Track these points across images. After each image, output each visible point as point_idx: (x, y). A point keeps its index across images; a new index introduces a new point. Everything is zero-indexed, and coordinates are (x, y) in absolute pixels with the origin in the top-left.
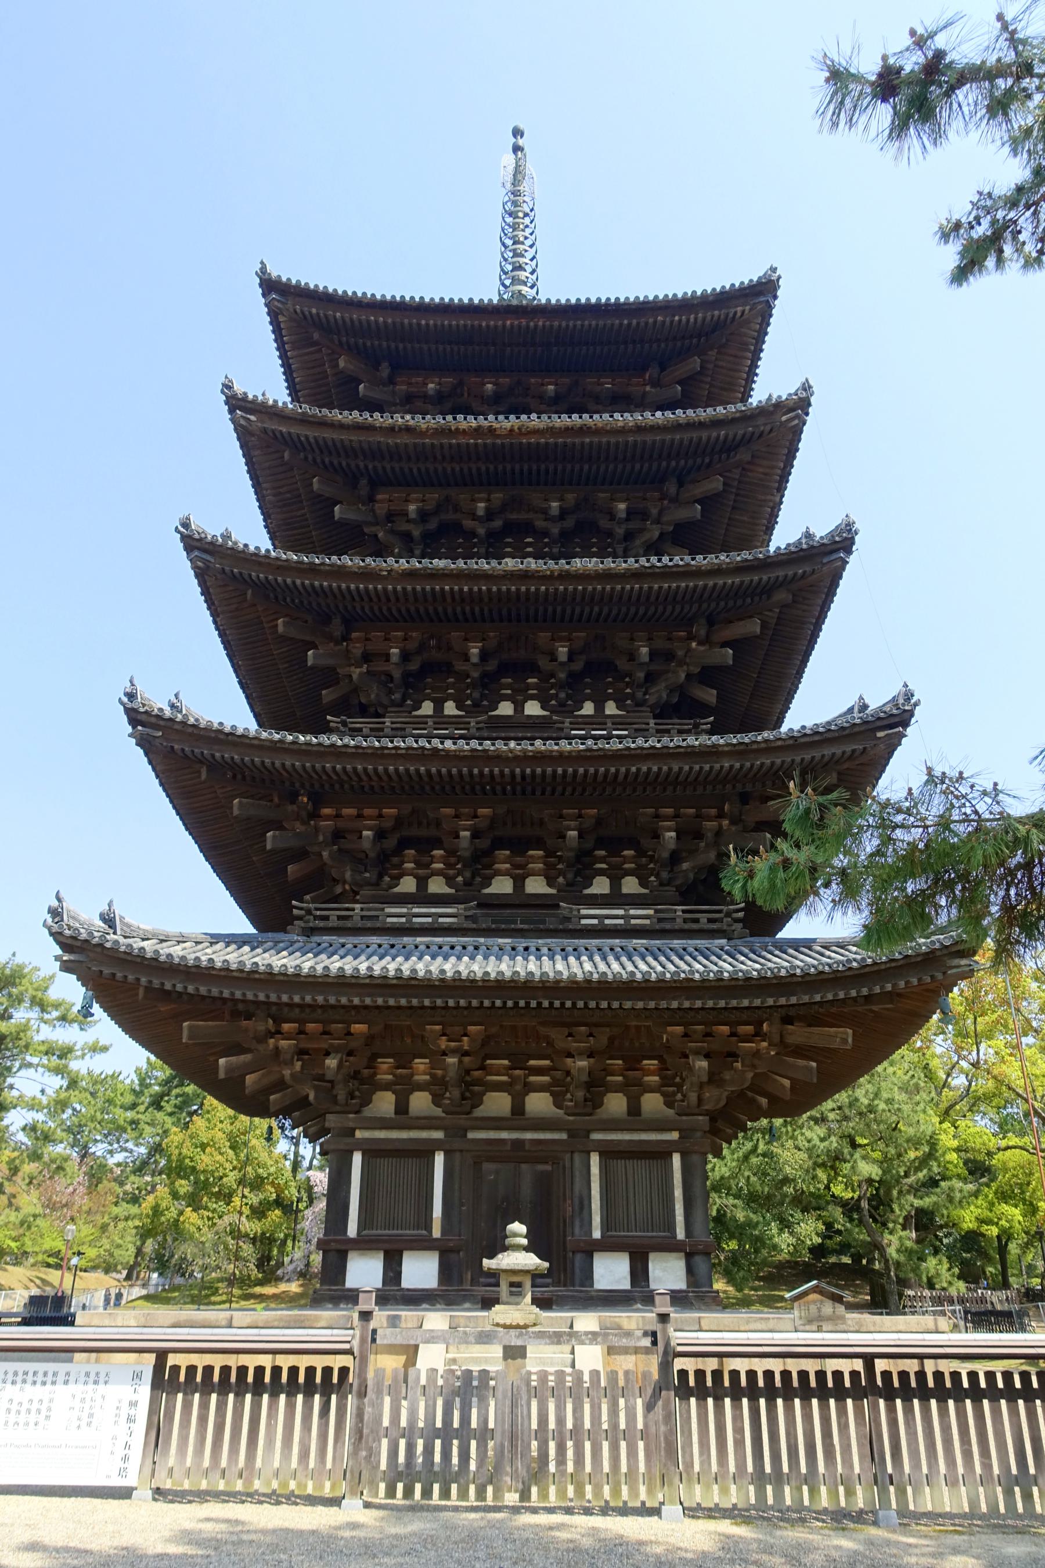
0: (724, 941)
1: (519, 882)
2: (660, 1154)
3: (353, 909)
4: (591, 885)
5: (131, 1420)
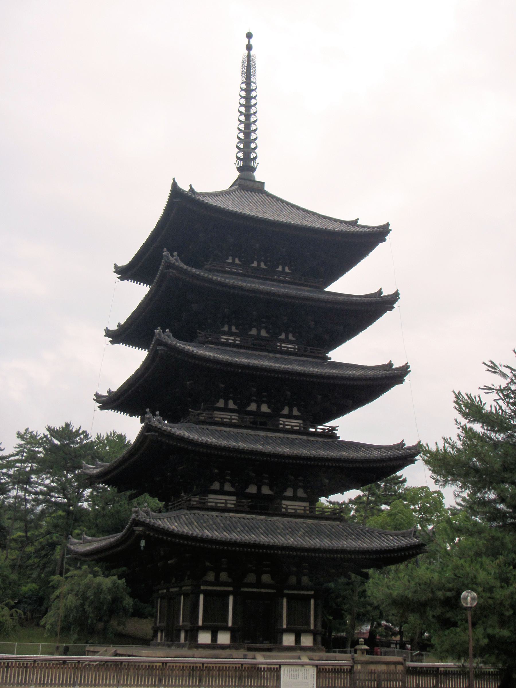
0: (338, 523)
1: (259, 489)
2: (307, 598)
3: (204, 499)
4: (285, 491)
5: (314, 678)
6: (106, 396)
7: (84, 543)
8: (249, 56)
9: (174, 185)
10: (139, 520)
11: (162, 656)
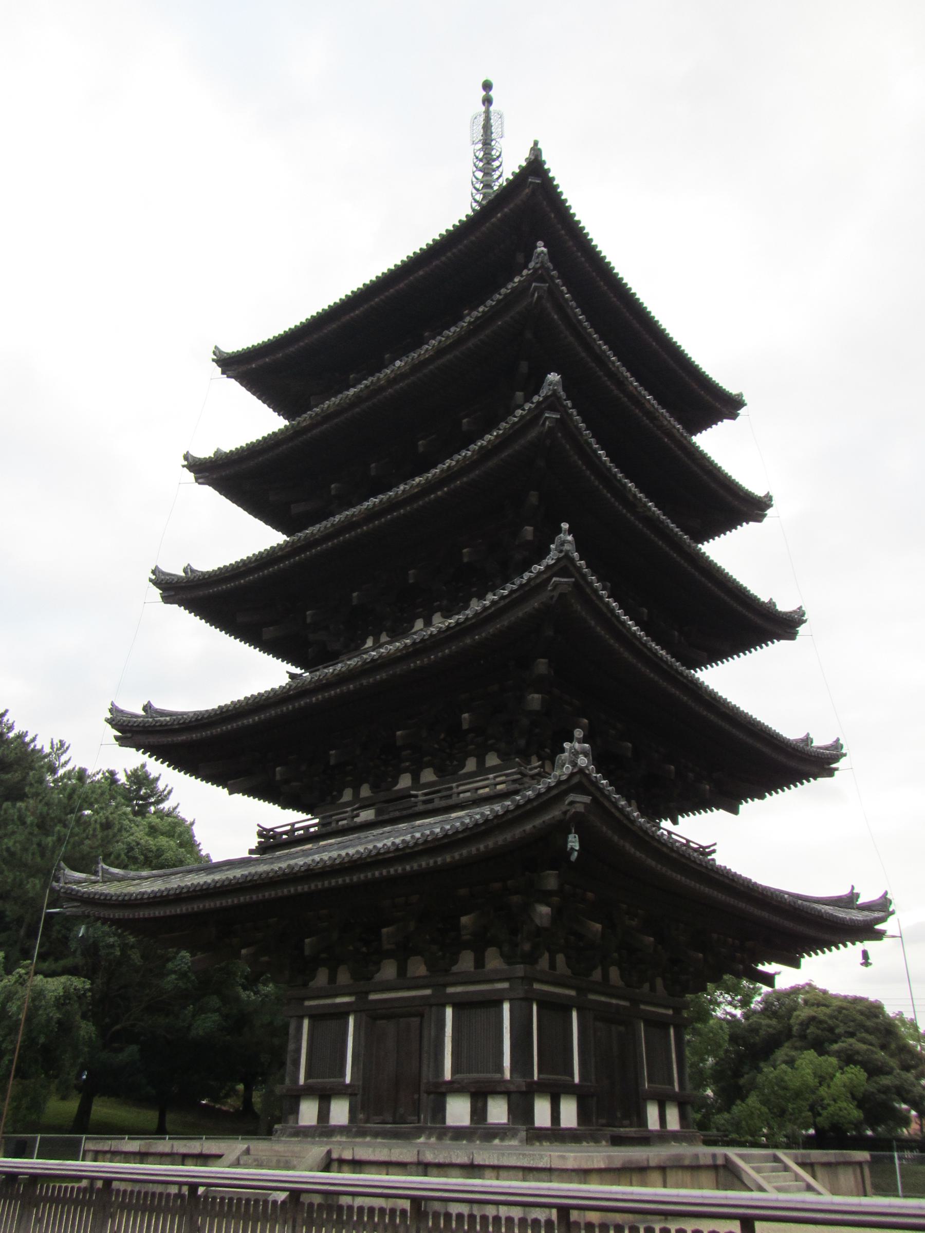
6: (181, 577)
7: (104, 882)
10: (588, 776)
11: (602, 1166)
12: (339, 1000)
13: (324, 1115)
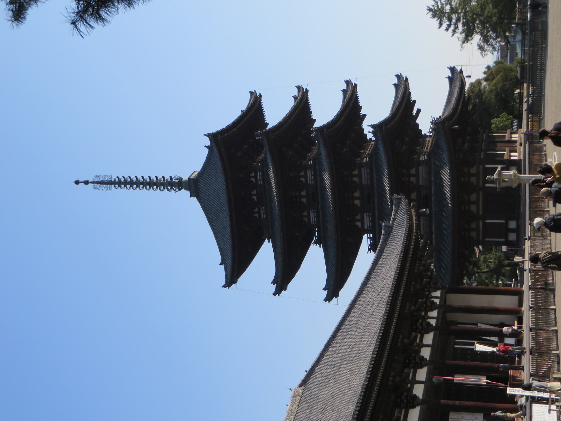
8: (93, 183)
9: (208, 135)
12: (481, 226)
13: (513, 231)
